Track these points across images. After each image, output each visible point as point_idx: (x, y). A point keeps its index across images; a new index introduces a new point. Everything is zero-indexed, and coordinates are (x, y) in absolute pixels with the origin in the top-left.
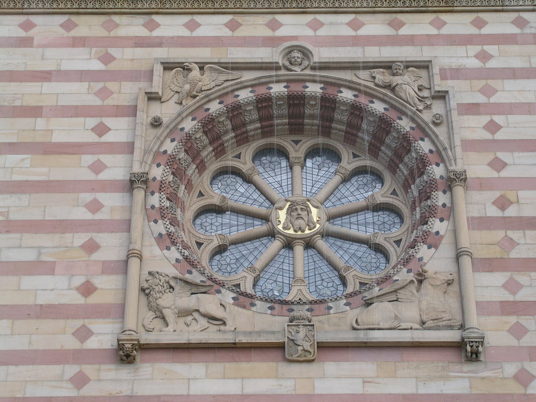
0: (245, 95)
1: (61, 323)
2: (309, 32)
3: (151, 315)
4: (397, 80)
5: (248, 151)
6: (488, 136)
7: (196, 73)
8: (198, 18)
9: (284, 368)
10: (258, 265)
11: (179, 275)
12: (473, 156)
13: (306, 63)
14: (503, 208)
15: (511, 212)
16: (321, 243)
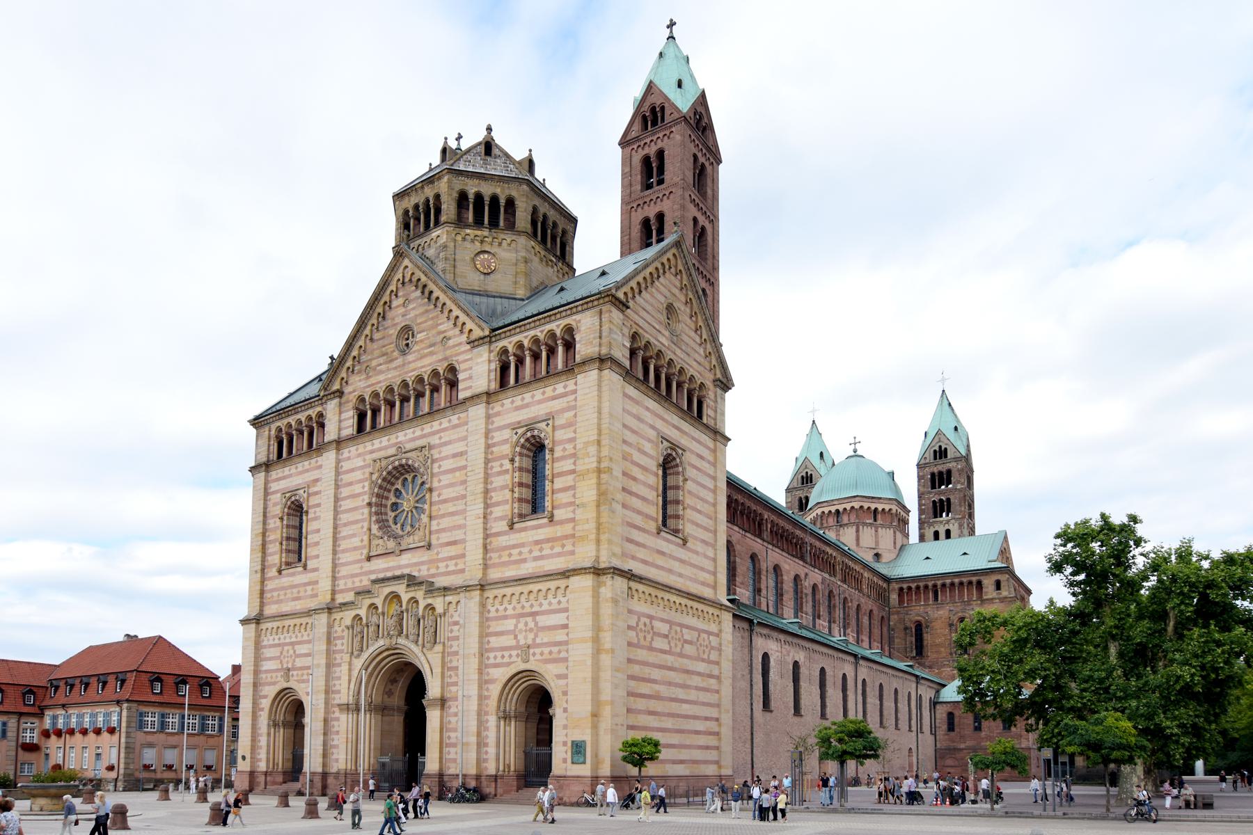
0: (390, 467)
5: (400, 481)
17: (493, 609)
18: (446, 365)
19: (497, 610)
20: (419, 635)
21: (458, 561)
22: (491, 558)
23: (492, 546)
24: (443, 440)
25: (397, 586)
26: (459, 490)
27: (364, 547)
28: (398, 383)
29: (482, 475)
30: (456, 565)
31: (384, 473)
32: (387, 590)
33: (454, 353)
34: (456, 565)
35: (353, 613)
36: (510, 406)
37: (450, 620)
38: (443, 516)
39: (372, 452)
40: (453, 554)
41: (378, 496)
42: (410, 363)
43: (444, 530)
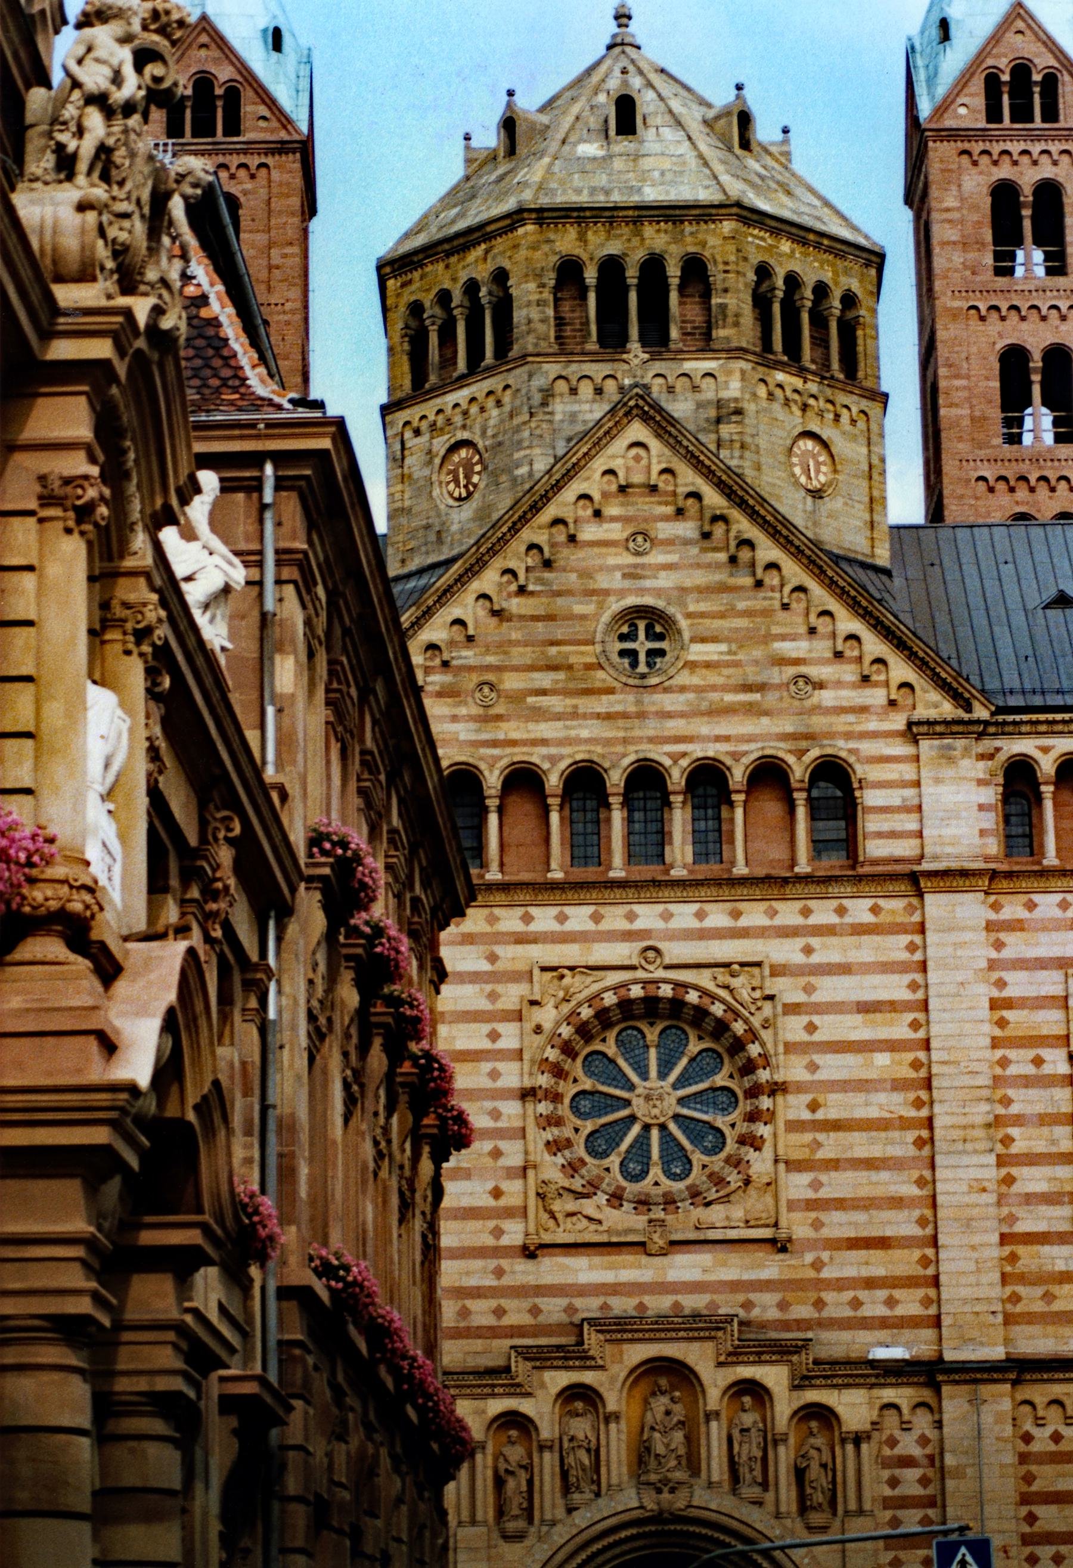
0: (610, 999)
1: (478, 1224)
2: (660, 924)
3: (546, 1216)
4: (735, 983)
5: (612, 1035)
6: (806, 1037)
7: (567, 981)
8: (568, 910)
9: (644, 1259)
10: (624, 1146)
11: (567, 1185)
12: (793, 1058)
13: (659, 961)
14: (813, 1111)
15: (820, 1115)
16: (672, 1127)
17: (1042, 1434)
18: (815, 753)
19: (1056, 1437)
20: (765, 1485)
21: (897, 1293)
22: (1015, 1298)
23: (1021, 1266)
24: (815, 959)
25: (683, 1345)
26: (897, 1104)
27: (509, 1213)
28: (626, 761)
29: (984, 1080)
30: (891, 1302)
31: (586, 1013)
32: (638, 1353)
33: (841, 728)
34: (891, 1302)
35: (496, 1406)
36: (1058, 913)
37: (887, 1451)
38: (834, 1165)
39: (521, 939)
40: (880, 1272)
41: (559, 1072)
42: (669, 715)
43: (840, 1204)
